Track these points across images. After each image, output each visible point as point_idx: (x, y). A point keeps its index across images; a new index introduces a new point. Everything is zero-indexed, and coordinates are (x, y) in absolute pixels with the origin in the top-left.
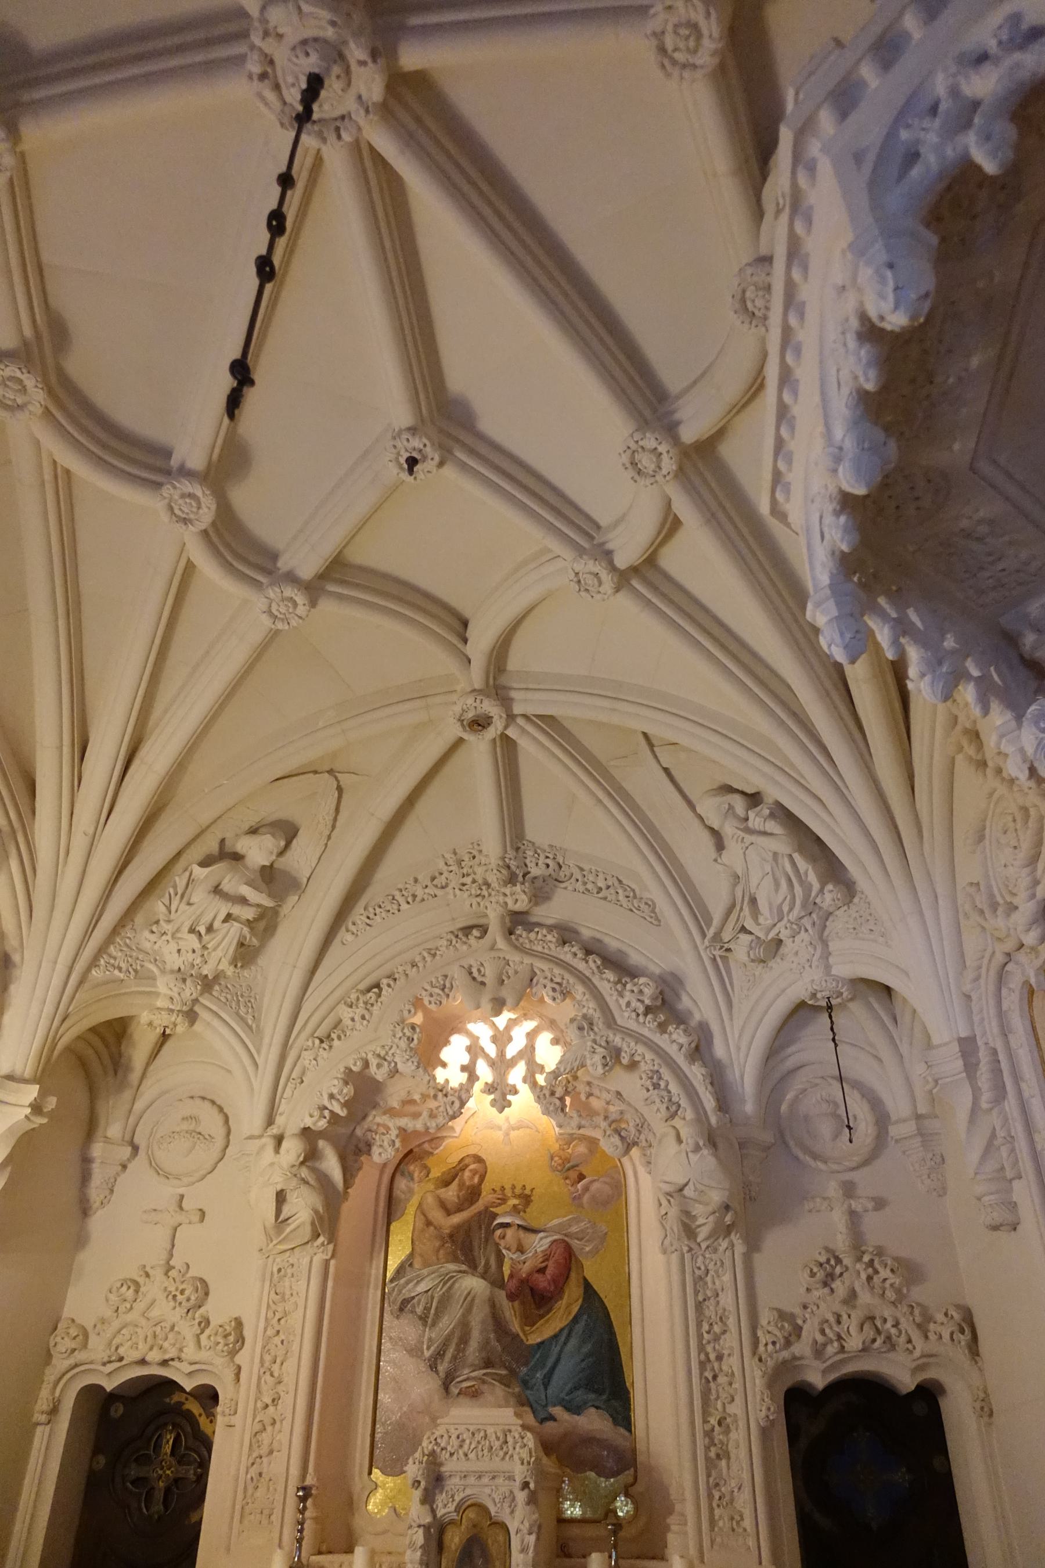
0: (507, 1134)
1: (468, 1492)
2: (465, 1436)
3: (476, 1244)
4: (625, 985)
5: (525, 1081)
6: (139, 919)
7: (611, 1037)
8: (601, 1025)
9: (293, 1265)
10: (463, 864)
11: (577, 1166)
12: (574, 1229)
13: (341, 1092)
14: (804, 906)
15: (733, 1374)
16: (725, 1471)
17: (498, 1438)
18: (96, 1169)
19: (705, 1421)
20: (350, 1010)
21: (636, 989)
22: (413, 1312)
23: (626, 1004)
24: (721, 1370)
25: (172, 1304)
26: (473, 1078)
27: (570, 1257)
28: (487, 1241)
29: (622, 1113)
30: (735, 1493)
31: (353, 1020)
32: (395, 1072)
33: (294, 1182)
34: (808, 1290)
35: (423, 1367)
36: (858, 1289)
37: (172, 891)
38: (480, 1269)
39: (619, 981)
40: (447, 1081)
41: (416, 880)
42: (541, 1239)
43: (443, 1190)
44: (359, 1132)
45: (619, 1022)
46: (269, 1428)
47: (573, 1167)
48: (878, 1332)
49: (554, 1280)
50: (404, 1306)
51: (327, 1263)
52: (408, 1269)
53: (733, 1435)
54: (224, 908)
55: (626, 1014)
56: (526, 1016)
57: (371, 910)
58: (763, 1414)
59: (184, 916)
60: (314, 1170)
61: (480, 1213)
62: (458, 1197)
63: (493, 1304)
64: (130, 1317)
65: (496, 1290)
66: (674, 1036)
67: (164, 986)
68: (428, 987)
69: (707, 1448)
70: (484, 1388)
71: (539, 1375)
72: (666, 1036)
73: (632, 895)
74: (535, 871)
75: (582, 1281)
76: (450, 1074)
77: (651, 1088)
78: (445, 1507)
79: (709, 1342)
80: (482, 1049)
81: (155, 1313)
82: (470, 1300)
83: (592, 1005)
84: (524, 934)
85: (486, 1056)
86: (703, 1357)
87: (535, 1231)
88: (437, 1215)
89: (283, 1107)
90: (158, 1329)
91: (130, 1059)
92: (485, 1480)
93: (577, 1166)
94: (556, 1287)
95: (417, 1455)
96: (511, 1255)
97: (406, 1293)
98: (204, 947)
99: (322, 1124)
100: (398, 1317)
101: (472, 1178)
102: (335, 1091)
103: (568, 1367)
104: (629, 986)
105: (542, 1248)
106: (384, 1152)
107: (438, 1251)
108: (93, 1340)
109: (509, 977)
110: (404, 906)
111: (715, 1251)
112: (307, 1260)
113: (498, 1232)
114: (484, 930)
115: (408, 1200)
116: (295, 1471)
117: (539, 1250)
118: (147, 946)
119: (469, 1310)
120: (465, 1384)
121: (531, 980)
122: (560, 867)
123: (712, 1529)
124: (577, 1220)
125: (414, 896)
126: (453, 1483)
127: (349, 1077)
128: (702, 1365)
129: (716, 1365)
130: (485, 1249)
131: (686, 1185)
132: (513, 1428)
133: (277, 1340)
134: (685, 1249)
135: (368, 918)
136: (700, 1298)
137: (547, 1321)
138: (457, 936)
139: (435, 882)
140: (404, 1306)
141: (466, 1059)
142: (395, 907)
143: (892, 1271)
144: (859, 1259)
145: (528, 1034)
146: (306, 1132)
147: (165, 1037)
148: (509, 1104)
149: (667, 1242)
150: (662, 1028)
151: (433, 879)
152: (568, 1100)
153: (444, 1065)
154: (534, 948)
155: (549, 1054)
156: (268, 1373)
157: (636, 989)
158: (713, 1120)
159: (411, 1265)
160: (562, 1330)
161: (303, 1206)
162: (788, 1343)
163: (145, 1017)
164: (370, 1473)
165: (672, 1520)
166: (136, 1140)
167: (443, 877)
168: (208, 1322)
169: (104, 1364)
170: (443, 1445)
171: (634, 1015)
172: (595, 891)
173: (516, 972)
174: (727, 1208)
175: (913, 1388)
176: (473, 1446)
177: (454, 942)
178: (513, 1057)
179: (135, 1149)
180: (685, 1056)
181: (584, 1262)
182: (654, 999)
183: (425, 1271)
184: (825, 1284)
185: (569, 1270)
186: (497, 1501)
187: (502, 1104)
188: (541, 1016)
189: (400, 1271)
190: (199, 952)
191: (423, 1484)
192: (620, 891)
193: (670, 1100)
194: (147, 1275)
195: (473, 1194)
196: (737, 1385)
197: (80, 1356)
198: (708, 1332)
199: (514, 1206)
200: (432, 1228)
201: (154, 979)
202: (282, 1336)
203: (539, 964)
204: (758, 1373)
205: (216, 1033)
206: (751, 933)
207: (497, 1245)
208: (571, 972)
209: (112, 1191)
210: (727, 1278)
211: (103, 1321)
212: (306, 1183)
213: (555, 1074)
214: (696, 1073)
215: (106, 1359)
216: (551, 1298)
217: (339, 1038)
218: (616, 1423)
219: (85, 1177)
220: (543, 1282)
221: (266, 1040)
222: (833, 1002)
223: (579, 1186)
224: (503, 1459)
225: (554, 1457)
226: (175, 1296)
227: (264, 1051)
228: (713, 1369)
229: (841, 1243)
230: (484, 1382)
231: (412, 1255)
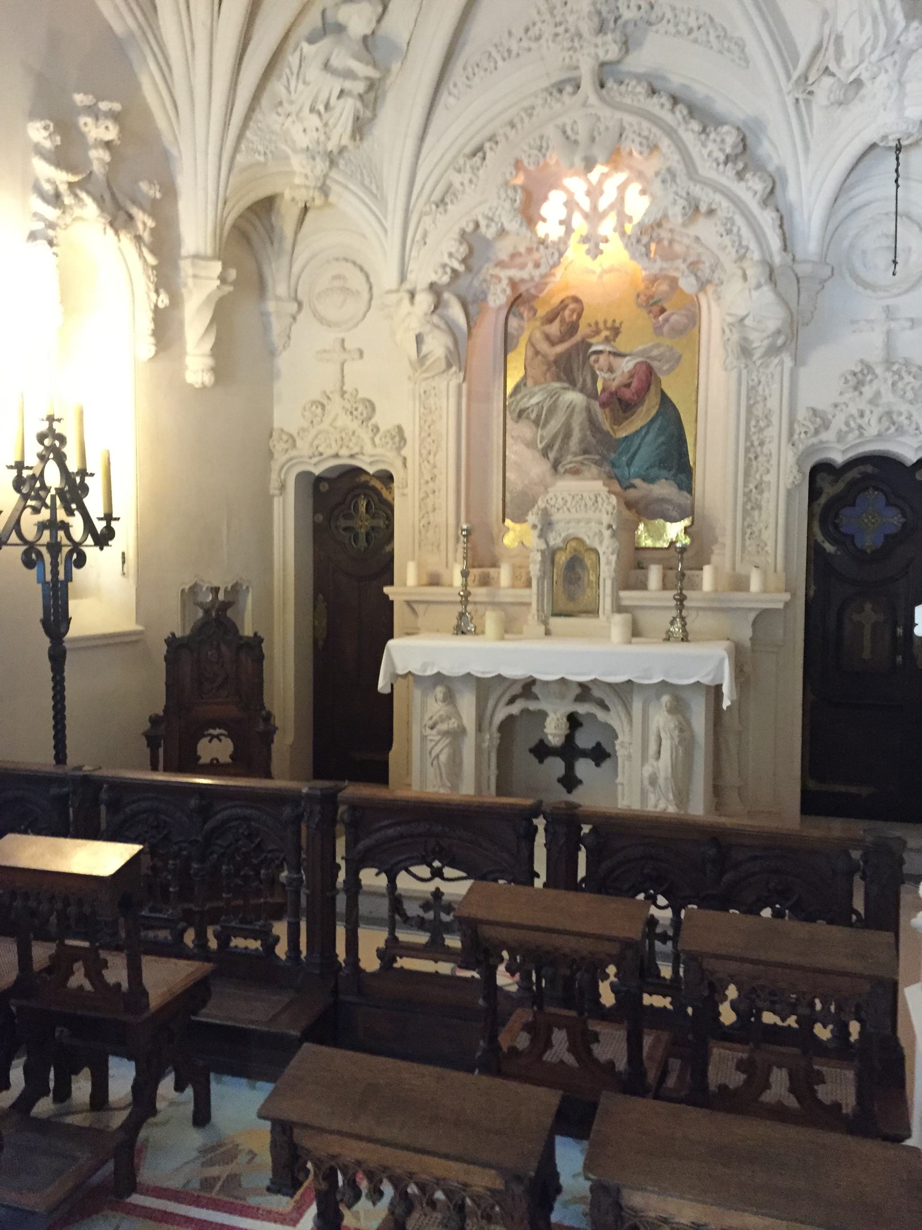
0: (600, 277)
3: (575, 366)
4: (708, 135)
5: (615, 230)
6: (265, 101)
8: (684, 178)
9: (434, 388)
10: (555, 12)
11: (660, 300)
12: (655, 353)
13: (458, 251)
14: (886, 45)
15: (771, 454)
16: (756, 518)
18: (274, 320)
19: (745, 486)
22: (528, 418)
23: (707, 153)
24: (762, 452)
25: (350, 417)
26: (569, 231)
27: (651, 374)
28: (584, 363)
29: (699, 255)
31: (462, 184)
32: (502, 232)
33: (428, 328)
34: (841, 394)
35: (538, 455)
36: (883, 391)
37: (288, 71)
38: (579, 385)
39: (704, 130)
40: (547, 235)
41: (510, 34)
44: (476, 283)
45: (701, 171)
46: (431, 496)
47: (655, 303)
48: (894, 423)
50: (521, 414)
51: (459, 387)
53: (766, 495)
54: (337, 85)
55: (708, 164)
56: (616, 168)
57: (470, 69)
58: (790, 480)
59: (303, 95)
60: (442, 317)
63: (588, 410)
64: (321, 427)
66: (750, 184)
67: (298, 163)
69: (745, 504)
70: (583, 468)
71: (624, 459)
72: (742, 184)
73: (724, 35)
74: (627, 15)
76: (549, 230)
77: (724, 234)
78: (555, 540)
79: (754, 433)
80: (577, 204)
81: (339, 423)
83: (676, 157)
84: (615, 86)
85: (582, 211)
86: (748, 444)
87: (623, 356)
88: (544, 347)
89: (412, 266)
90: (344, 435)
91: (282, 229)
92: (582, 524)
94: (638, 397)
95: (535, 510)
97: (522, 405)
98: (326, 125)
99: (446, 279)
100: (517, 422)
101: (571, 316)
102: (453, 250)
103: (646, 453)
104: (712, 136)
106: (498, 298)
107: (545, 374)
108: (299, 443)
110: (500, 63)
111: (767, 366)
112: (445, 383)
113: (593, 358)
116: (452, 521)
118: (277, 127)
120: (568, 467)
121: (621, 135)
122: (652, 7)
124: (657, 346)
125: (509, 51)
126: (559, 527)
127: (463, 236)
128: (747, 450)
129: (759, 449)
130: (583, 369)
131: (747, 316)
133: (429, 440)
134: (743, 366)
135: (468, 78)
136: (752, 402)
137: (632, 422)
138: (551, 94)
139: (530, 33)
140: (521, 414)
141: (563, 215)
142: (492, 65)
143: (914, 377)
144: (888, 369)
145: (619, 188)
146: (433, 287)
147: (306, 209)
148: (601, 252)
149: (728, 361)
150: (740, 176)
151: (527, 30)
152: (653, 247)
153: (544, 220)
155: (638, 206)
156: (426, 463)
157: (718, 139)
158: (777, 260)
159: (525, 384)
160: (642, 428)
161: (437, 345)
162: (817, 432)
163: (287, 195)
164: (504, 521)
165: (716, 549)
166: (300, 296)
167: (537, 27)
168: (378, 429)
169: (311, 458)
170: (552, 503)
171: (715, 165)
172: (686, 33)
173: (607, 128)
174: (779, 332)
175: (915, 461)
177: (549, 100)
178: (604, 211)
179: (300, 305)
180: (759, 203)
181: (661, 377)
182: (734, 146)
183: (537, 389)
184: (856, 388)
185: (649, 385)
186: (591, 536)
187: (595, 252)
188: (630, 168)
189: (517, 389)
190: (321, 130)
191: (539, 527)
192: (711, 31)
193: (740, 244)
194: (329, 398)
195: (572, 329)
196: (774, 461)
197: (293, 453)
198: (755, 427)
200: (540, 357)
201: (287, 158)
202: (433, 437)
203: (628, 119)
204: (791, 454)
205: (348, 201)
206: (833, 75)
207: (592, 368)
209: (289, 337)
210: (775, 387)
211: (303, 430)
213: (641, 225)
214: (767, 219)
215: (311, 454)
216: (636, 405)
217: (452, 202)
218: (680, 488)
219: (266, 328)
220: (628, 394)
221: (390, 206)
222: (904, 143)
223: (661, 318)
224: (595, 511)
225: (634, 510)
226: (351, 413)
227: (390, 217)
228: (755, 452)
229: (875, 356)
230: (582, 464)
231: (525, 376)
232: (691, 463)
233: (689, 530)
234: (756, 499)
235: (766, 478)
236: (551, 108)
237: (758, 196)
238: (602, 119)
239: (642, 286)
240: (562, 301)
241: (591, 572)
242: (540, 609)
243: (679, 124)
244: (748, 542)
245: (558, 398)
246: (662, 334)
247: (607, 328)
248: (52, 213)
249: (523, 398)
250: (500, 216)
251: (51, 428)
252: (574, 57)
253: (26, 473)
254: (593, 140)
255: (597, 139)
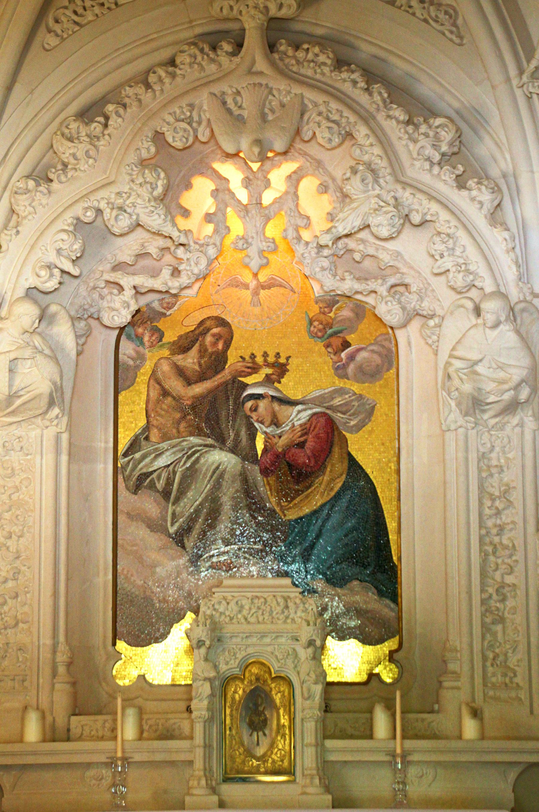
1: (250, 650)
2: (244, 602)
4: (417, 127)
7: (400, 193)
11: (340, 332)
12: (337, 401)
15: (514, 545)
16: (500, 635)
17: (278, 604)
19: (482, 591)
20: (70, 144)
21: (431, 134)
22: (152, 486)
26: (222, 229)
27: (333, 431)
28: (235, 413)
30: (509, 654)
31: (74, 155)
33: (28, 353)
38: (229, 443)
42: (299, 412)
43: (180, 357)
47: (335, 333)
49: (315, 456)
52: (143, 443)
53: (510, 603)
61: (225, 384)
62: (200, 365)
63: (244, 478)
65: (249, 466)
66: (474, 193)
68: (171, 119)
69: (483, 615)
72: (465, 193)
75: (345, 455)
79: (490, 517)
82: (219, 475)
83: (377, 150)
84: (290, 52)
88: (175, 385)
92: (267, 640)
93: (340, 332)
94: (316, 462)
96: (265, 429)
100: (135, 493)
101: (215, 344)
104: (423, 128)
105: (299, 422)
109: (273, 111)
111: (502, 429)
113: (249, 404)
114: (240, 45)
115: (138, 367)
117: (296, 424)
119: (218, 485)
123: (485, 685)
129: (496, 539)
130: (234, 420)
131: (481, 361)
132: (292, 595)
135: (75, 12)
137: (307, 497)
138: (202, 51)
140: (141, 483)
145: (289, 177)
146: (32, 294)
150: (461, 183)
153: (186, 213)
154: (303, 71)
157: (431, 134)
159: (147, 438)
160: (323, 506)
164: (114, 644)
170: (221, 609)
171: (427, 165)
176: (253, 611)
177: (199, 58)
181: (348, 435)
182: (451, 144)
183: (164, 445)
186: (280, 657)
189: (134, 445)
191: (208, 643)
195: (218, 362)
199: (267, 375)
200: (170, 399)
203: (310, 95)
207: (248, 417)
208: (350, 107)
212: (41, 352)
218: (381, 594)
220: (302, 458)
223: (343, 355)
224: (285, 622)
231: (147, 428)
232: (395, 558)
233: (396, 656)
234: (498, 609)
235: (509, 579)
236: (202, 69)
237: (485, 211)
238: (275, 92)
239: (314, 310)
240: (202, 323)
241: (281, 711)
242: (207, 771)
243: (378, 110)
244: (490, 669)
245: (197, 460)
246: (345, 376)
247: (267, 365)
249: (144, 457)
250: (134, 205)
252: (235, 8)
254: (263, 117)
255: (270, 118)
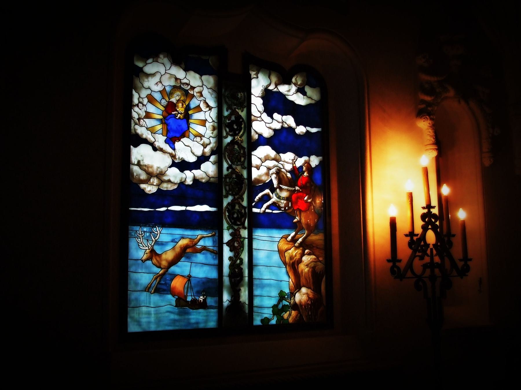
248: (428, 98)
251: (429, 212)
253: (415, 238)
